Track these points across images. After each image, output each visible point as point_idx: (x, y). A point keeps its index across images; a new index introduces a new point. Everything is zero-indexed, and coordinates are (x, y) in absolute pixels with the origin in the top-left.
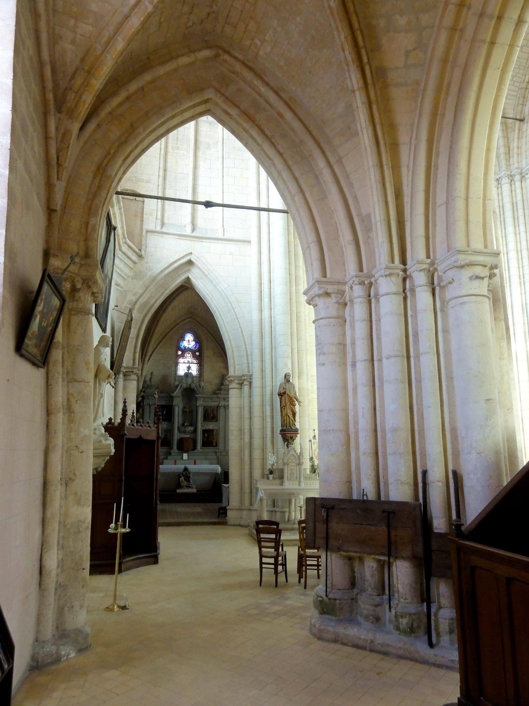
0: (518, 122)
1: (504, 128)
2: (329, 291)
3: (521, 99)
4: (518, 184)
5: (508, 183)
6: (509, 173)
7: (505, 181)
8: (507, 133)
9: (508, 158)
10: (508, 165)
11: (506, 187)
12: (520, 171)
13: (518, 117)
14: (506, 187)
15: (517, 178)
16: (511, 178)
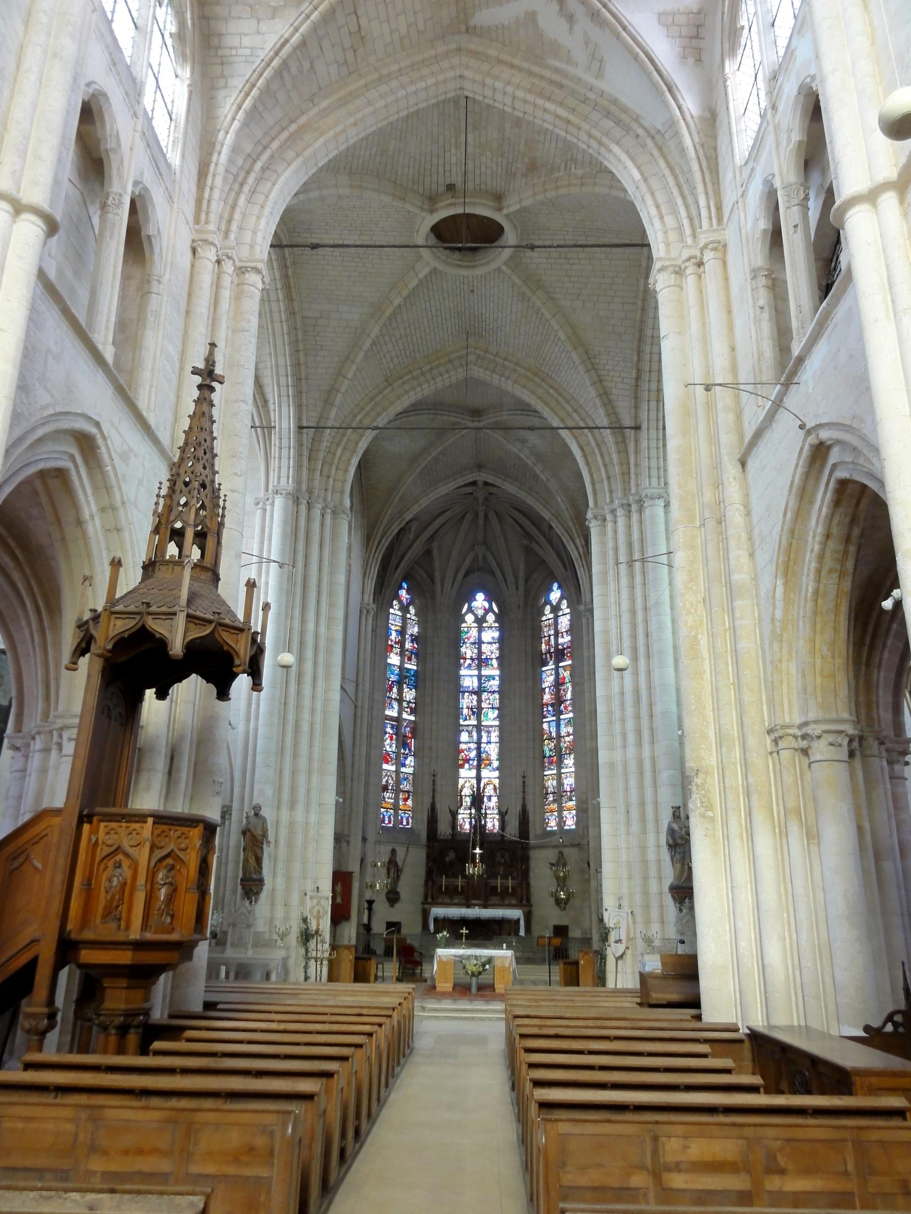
0: (633, 431)
1: (620, 439)
2: (18, 745)
3: (633, 401)
4: (635, 517)
5: (625, 516)
6: (625, 501)
7: (620, 512)
8: (626, 446)
9: (626, 479)
10: (626, 491)
11: (621, 521)
12: (637, 498)
13: (633, 425)
14: (621, 521)
15: (634, 507)
16: (626, 508)
